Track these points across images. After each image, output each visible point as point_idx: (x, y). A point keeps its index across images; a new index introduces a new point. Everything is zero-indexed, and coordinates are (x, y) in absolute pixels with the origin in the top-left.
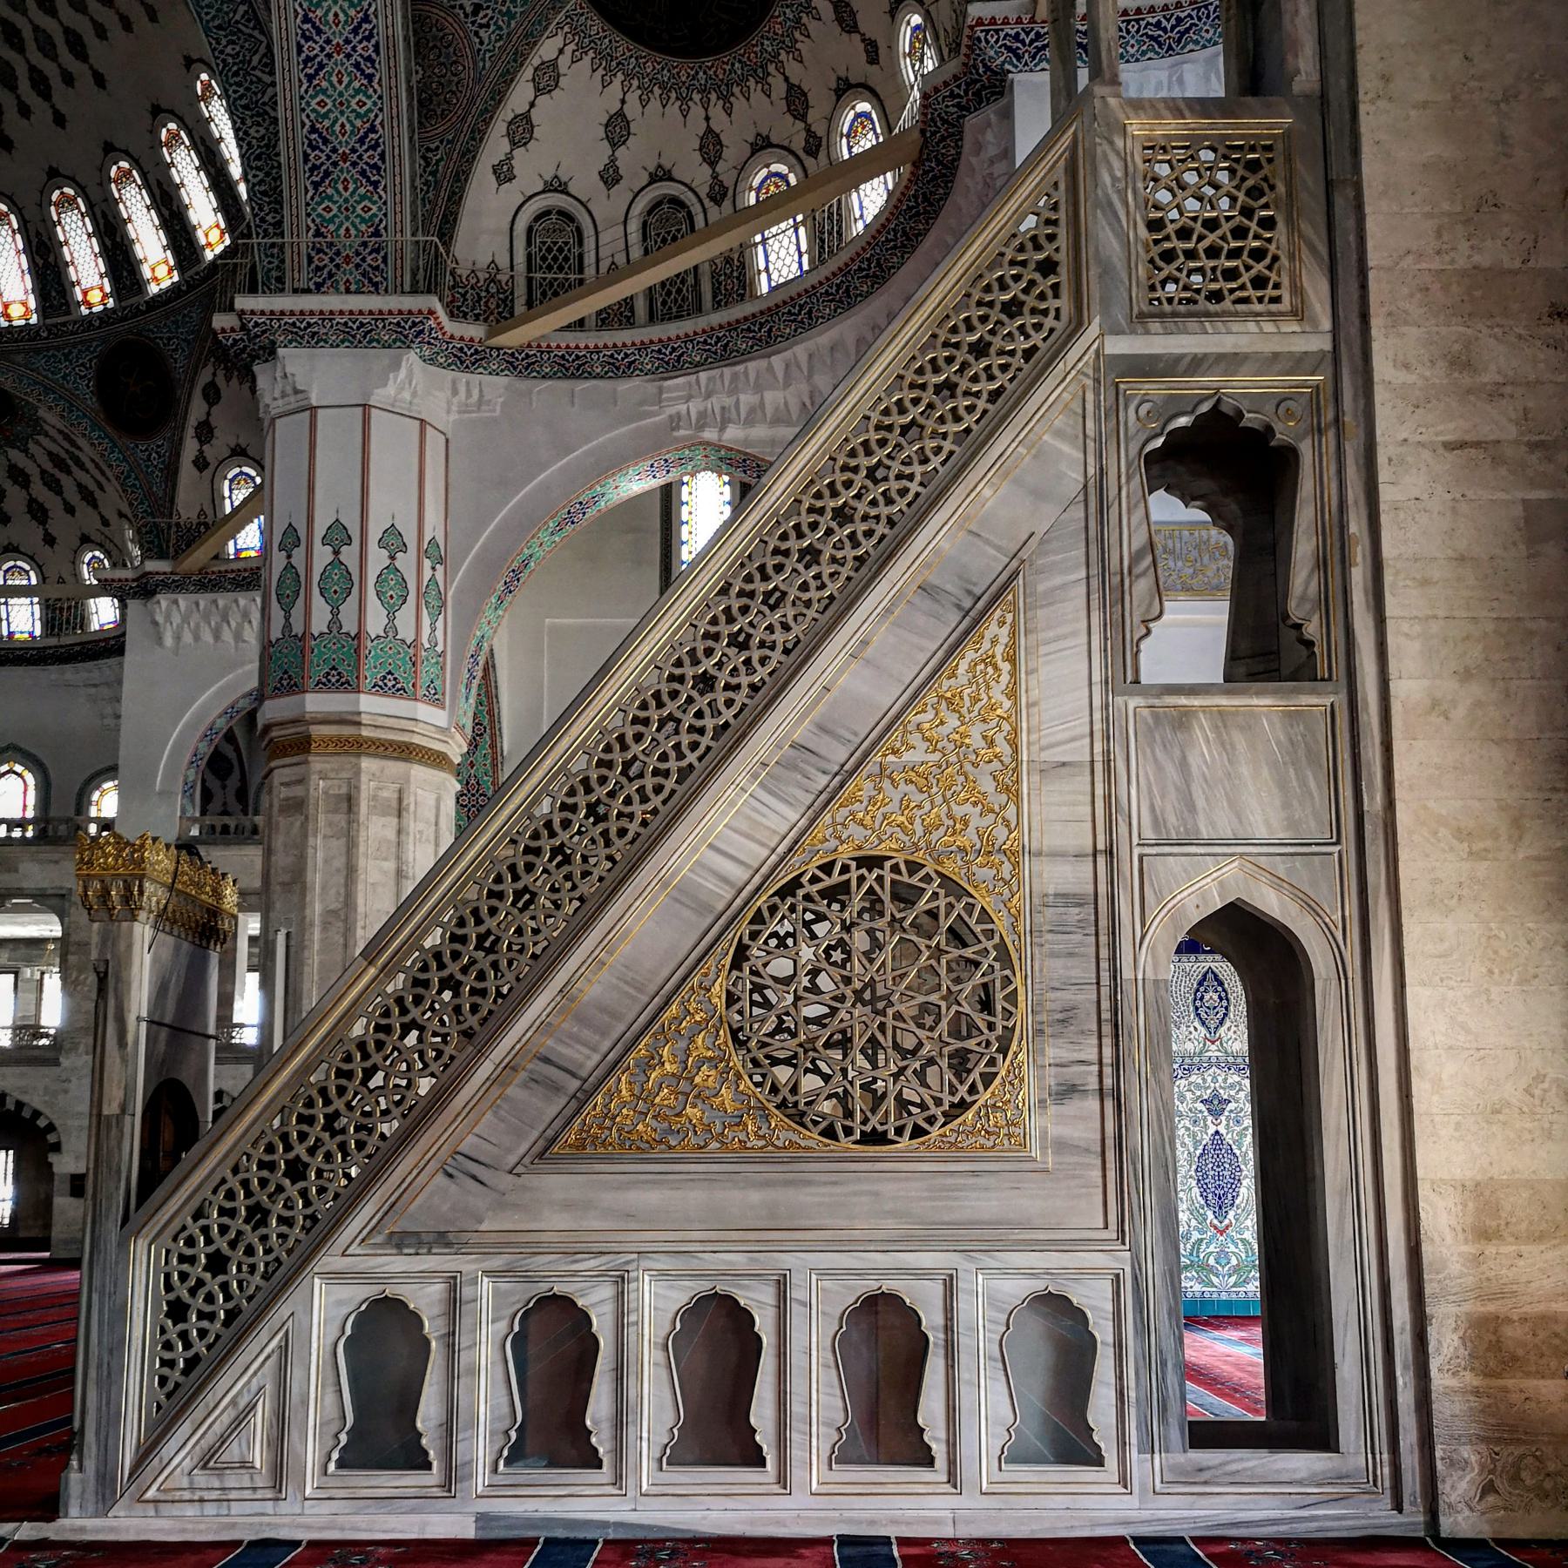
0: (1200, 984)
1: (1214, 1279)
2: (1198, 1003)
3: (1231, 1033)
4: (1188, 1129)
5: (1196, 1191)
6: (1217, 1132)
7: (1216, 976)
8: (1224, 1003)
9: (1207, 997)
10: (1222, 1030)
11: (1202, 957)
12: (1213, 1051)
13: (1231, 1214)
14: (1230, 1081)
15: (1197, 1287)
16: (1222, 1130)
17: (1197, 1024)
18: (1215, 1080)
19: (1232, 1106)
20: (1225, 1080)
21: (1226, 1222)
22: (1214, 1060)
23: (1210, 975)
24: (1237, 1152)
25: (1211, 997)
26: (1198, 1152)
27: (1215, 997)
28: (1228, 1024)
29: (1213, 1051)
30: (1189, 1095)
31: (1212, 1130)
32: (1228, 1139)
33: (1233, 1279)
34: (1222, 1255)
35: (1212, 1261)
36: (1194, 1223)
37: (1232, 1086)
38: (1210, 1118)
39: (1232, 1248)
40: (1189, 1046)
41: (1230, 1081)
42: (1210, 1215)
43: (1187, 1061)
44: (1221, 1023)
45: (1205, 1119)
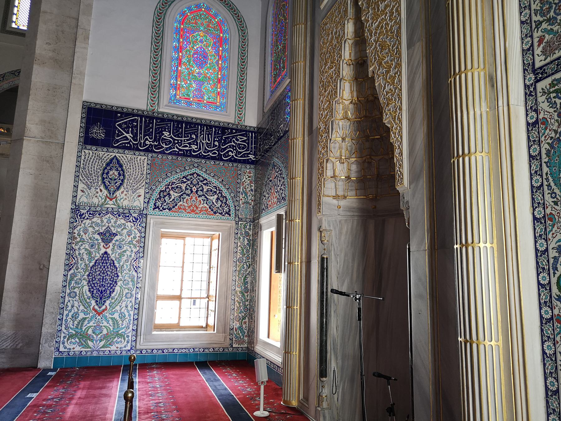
0: (108, 165)
1: (90, 343)
2: (105, 176)
3: (123, 195)
4: (86, 250)
5: (86, 288)
6: (106, 253)
7: (118, 161)
8: (122, 177)
9: (111, 173)
10: (118, 193)
11: (111, 150)
12: (110, 204)
13: (108, 302)
14: (119, 222)
15: (78, 349)
16: (109, 251)
17: (102, 188)
18: (109, 221)
19: (117, 238)
20: (115, 223)
21: (104, 307)
22: (110, 210)
23: (115, 160)
24: (117, 265)
25: (114, 173)
26: (91, 264)
27: (116, 173)
28: (122, 189)
29: (110, 204)
30: (91, 229)
31: (103, 251)
32: (113, 257)
33: (102, 343)
34: (98, 328)
35: (90, 332)
36: (82, 308)
37: (119, 226)
38: (102, 244)
39: (105, 324)
40: (95, 201)
41: (119, 222)
42: (93, 302)
43: (93, 209)
44: (118, 188)
45: (99, 244)
